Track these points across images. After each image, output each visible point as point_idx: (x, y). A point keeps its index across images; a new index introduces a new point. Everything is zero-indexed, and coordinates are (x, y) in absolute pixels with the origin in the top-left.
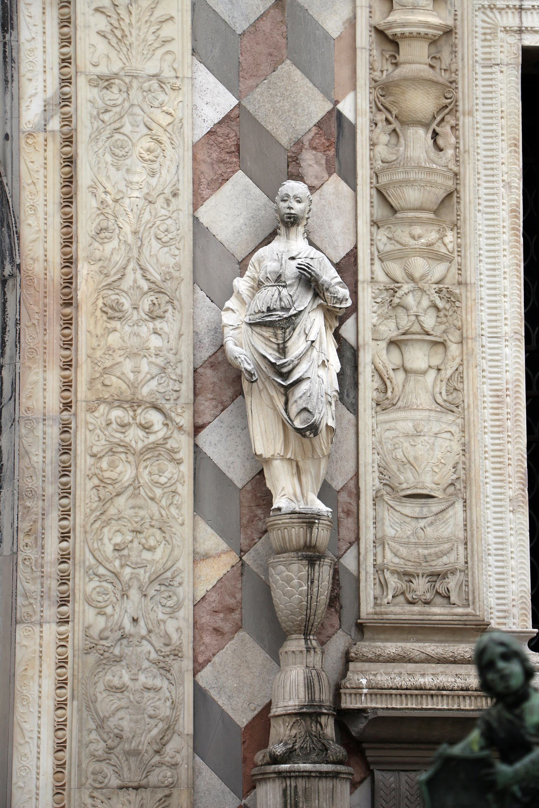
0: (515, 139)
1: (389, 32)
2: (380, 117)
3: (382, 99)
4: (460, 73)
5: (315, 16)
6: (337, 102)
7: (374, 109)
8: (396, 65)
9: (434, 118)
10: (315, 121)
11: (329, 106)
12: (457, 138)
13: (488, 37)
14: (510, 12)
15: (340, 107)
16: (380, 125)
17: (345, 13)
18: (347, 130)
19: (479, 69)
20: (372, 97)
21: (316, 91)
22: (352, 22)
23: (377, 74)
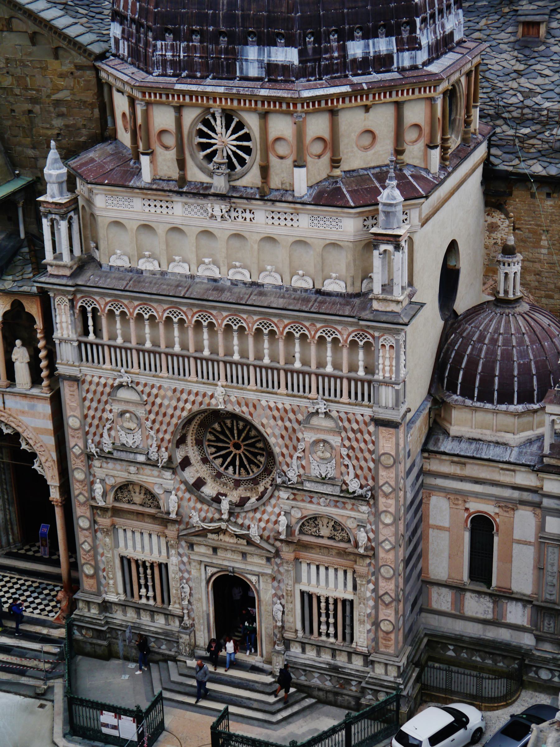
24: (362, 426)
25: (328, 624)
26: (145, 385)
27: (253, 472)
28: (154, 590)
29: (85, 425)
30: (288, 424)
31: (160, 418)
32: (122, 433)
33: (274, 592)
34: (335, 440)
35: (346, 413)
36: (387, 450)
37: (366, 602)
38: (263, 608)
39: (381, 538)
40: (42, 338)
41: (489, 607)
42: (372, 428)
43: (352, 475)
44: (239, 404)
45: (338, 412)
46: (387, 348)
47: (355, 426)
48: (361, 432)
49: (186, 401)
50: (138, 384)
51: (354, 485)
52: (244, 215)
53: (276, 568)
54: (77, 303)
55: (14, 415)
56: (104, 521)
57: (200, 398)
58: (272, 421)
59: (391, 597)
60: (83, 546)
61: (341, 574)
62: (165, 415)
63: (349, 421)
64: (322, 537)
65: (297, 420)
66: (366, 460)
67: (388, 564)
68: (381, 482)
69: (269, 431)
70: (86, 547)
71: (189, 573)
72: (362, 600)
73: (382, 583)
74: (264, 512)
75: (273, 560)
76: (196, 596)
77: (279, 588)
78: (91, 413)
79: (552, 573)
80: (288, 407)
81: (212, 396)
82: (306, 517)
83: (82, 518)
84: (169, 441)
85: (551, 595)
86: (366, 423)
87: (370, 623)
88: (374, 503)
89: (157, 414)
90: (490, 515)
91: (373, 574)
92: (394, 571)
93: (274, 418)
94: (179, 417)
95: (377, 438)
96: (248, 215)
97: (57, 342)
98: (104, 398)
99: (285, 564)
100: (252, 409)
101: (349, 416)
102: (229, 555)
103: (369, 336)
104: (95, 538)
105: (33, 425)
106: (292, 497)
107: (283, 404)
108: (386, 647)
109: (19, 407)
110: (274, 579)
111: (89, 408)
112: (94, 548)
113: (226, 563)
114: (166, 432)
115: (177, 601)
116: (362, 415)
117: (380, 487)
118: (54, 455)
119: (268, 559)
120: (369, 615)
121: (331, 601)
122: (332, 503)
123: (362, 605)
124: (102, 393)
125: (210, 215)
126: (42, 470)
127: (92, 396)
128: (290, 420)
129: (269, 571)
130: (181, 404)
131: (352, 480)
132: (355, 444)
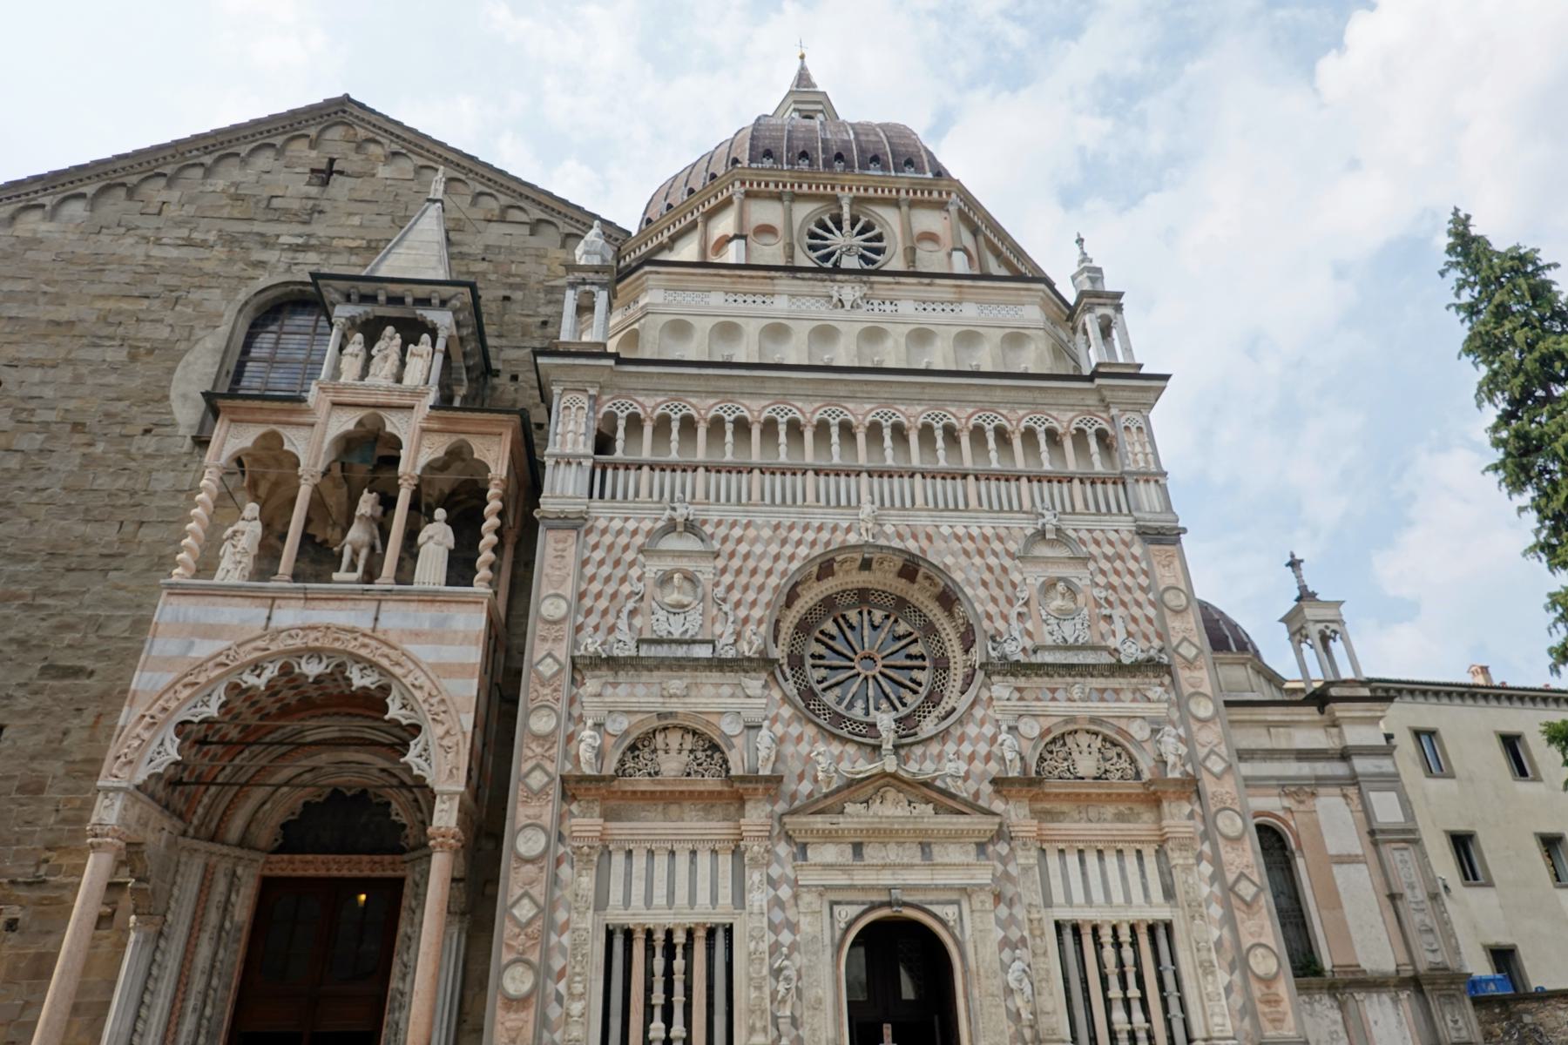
24: (1121, 549)
25: (1127, 1002)
26: (719, 524)
27: (904, 705)
28: (688, 1024)
29: (578, 611)
30: (992, 561)
31: (743, 579)
32: (662, 615)
33: (1001, 934)
34: (1080, 576)
35: (1089, 530)
36: (1171, 582)
37: (1204, 910)
38: (976, 993)
39: (1202, 752)
40: (495, 496)
41: (1335, 1022)
42: (1137, 549)
43: (1121, 635)
44: (900, 536)
45: (1075, 530)
46: (1134, 430)
47: (1109, 551)
48: (1121, 558)
49: (799, 543)
50: (704, 522)
51: (1129, 651)
52: (882, 307)
53: (1000, 867)
54: (601, 406)
55: (393, 639)
56: (586, 823)
57: (825, 535)
58: (963, 560)
59: (1254, 883)
60: (516, 912)
61: (1131, 862)
62: (754, 572)
63: (1097, 543)
64: (1082, 778)
65: (1008, 553)
66: (1139, 604)
67: (1228, 805)
68: (1175, 642)
69: (958, 576)
70: (524, 911)
71: (793, 927)
72: (1195, 909)
73: (1227, 854)
74: (961, 739)
75: (990, 848)
76: (810, 995)
77: (1012, 920)
78: (596, 587)
79: (1417, 903)
80: (989, 532)
81: (848, 530)
82: (1049, 731)
83: (529, 832)
84: (760, 622)
85: (1434, 951)
86: (1124, 543)
87: (1225, 965)
88: (1173, 681)
89: (739, 572)
90: (1278, 818)
91: (1205, 836)
92: (1244, 820)
93: (966, 553)
94: (784, 573)
95: (1149, 563)
96: (888, 307)
97: (549, 462)
98: (630, 556)
99: (1019, 853)
100: (924, 543)
101: (1095, 534)
102: (893, 854)
103: (1100, 421)
104: (555, 881)
105: (430, 661)
106: (1016, 695)
107: (980, 527)
108: (1277, 1021)
109: (410, 624)
110: (998, 898)
111: (592, 579)
112: (546, 910)
113: (887, 878)
114: (754, 604)
115: (759, 1025)
116: (1116, 531)
117: (1175, 650)
118: (468, 721)
119: (981, 847)
120: (1219, 944)
121: (1125, 936)
122: (1095, 695)
123: (1198, 922)
124: (626, 548)
125: (835, 300)
126: (424, 765)
127: (603, 555)
128: (995, 554)
129: (983, 876)
130: (788, 550)
131: (1124, 642)
132: (1115, 580)
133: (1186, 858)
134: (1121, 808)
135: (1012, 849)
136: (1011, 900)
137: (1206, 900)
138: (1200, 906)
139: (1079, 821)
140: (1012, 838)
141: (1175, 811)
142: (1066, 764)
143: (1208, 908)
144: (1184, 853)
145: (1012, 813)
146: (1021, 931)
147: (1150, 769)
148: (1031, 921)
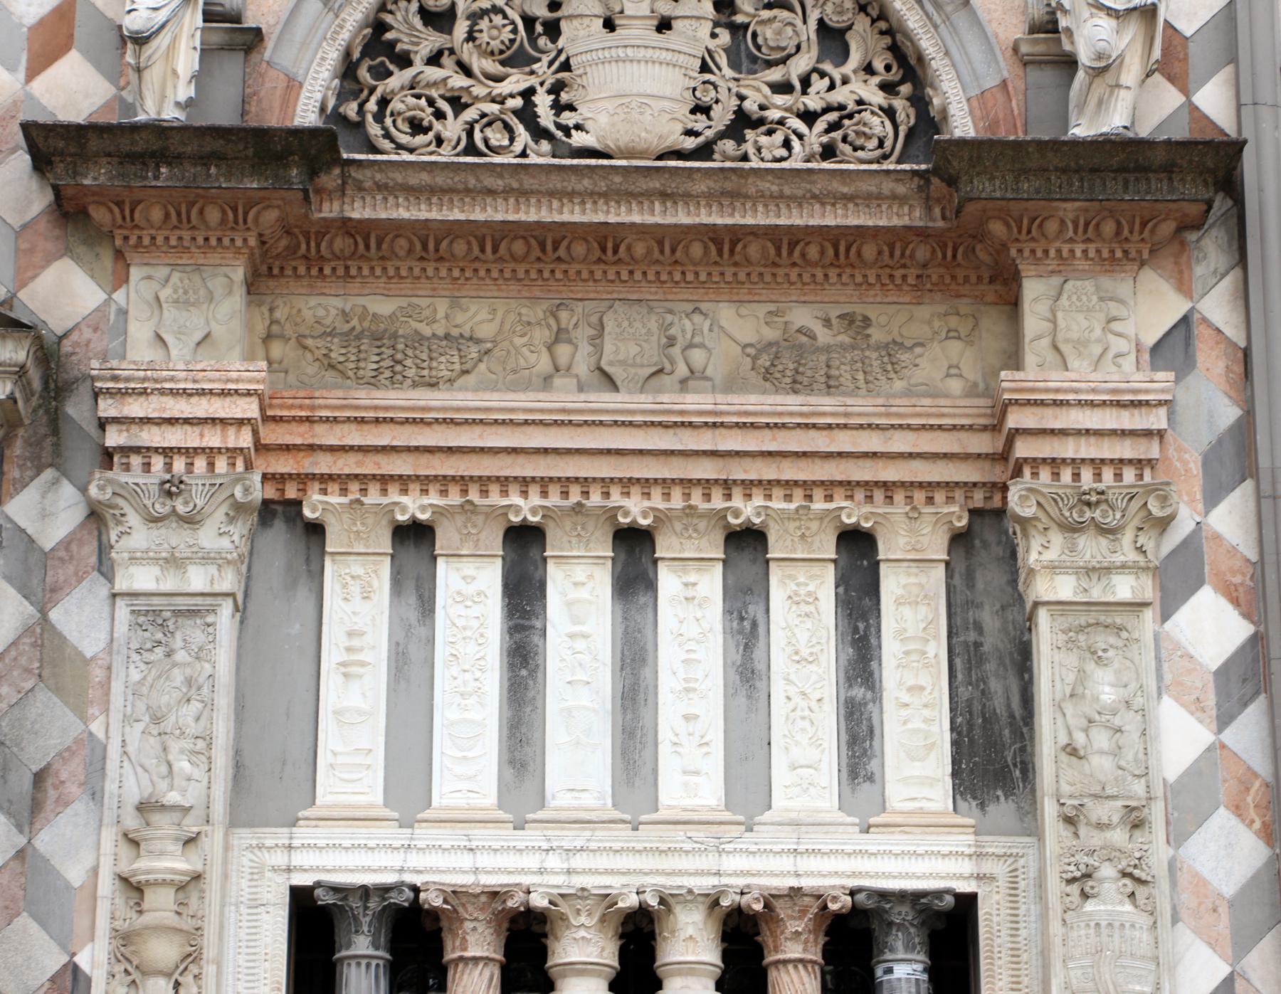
0: (278, 982)
1: (133, 880)
2: (119, 968)
3: (122, 949)
4: (206, 919)
5: (57, 866)
6: (74, 954)
7: (113, 960)
8: (140, 912)
9: (177, 967)
10: (49, 975)
11: (65, 959)
12: (200, 987)
13: (255, 877)
14: (279, 851)
15: (76, 959)
16: (117, 977)
17: (89, 862)
18: (82, 984)
19: (243, 910)
20: (111, 947)
21: (53, 944)
22: (95, 871)
23: (118, 924)
37: (1159, 853)
133: (1101, 571)
134: (802, 317)
135: (96, 516)
136: (39, 778)
137: (1174, 791)
138: (1136, 823)
139: (546, 382)
140: (107, 457)
141: (1074, 324)
142: (516, 81)
143: (1177, 837)
144: (1091, 548)
145: (139, 331)
146: (65, 942)
147: (979, 102)
148: (134, 888)
